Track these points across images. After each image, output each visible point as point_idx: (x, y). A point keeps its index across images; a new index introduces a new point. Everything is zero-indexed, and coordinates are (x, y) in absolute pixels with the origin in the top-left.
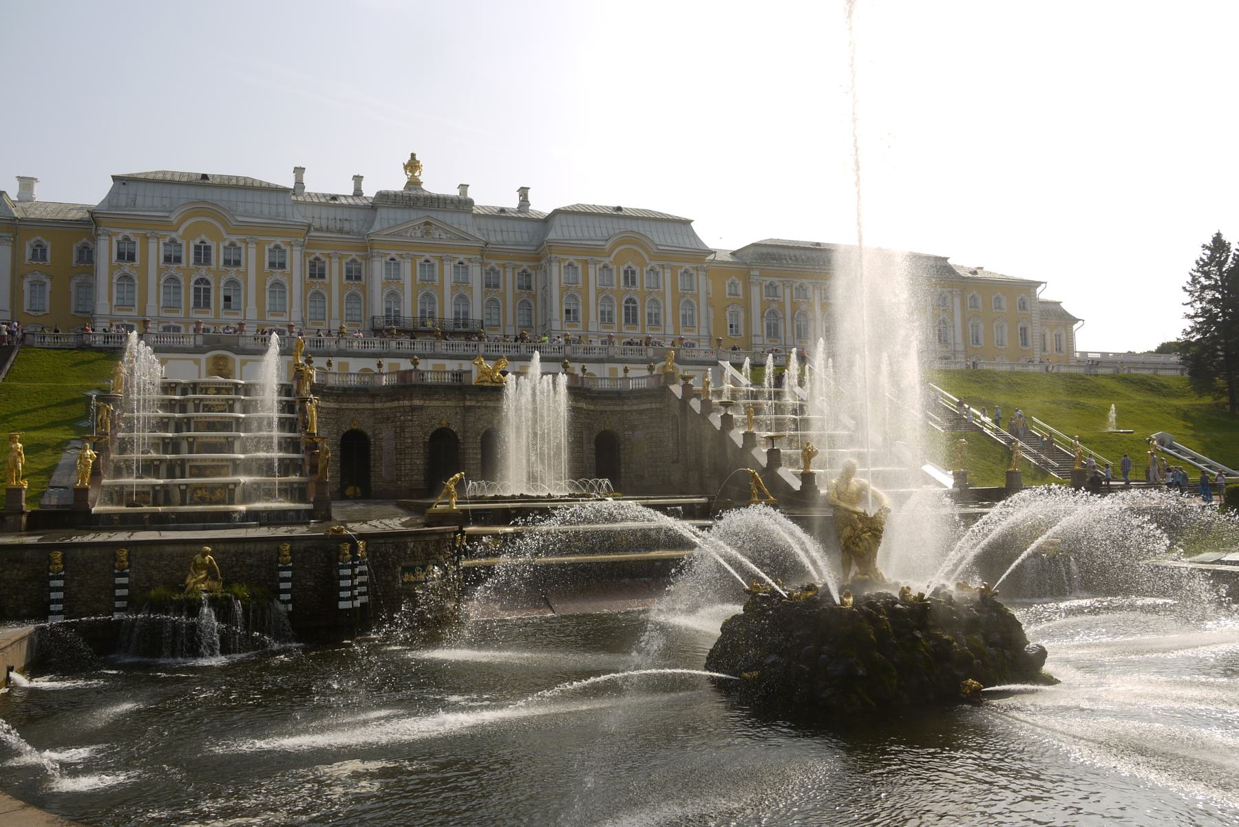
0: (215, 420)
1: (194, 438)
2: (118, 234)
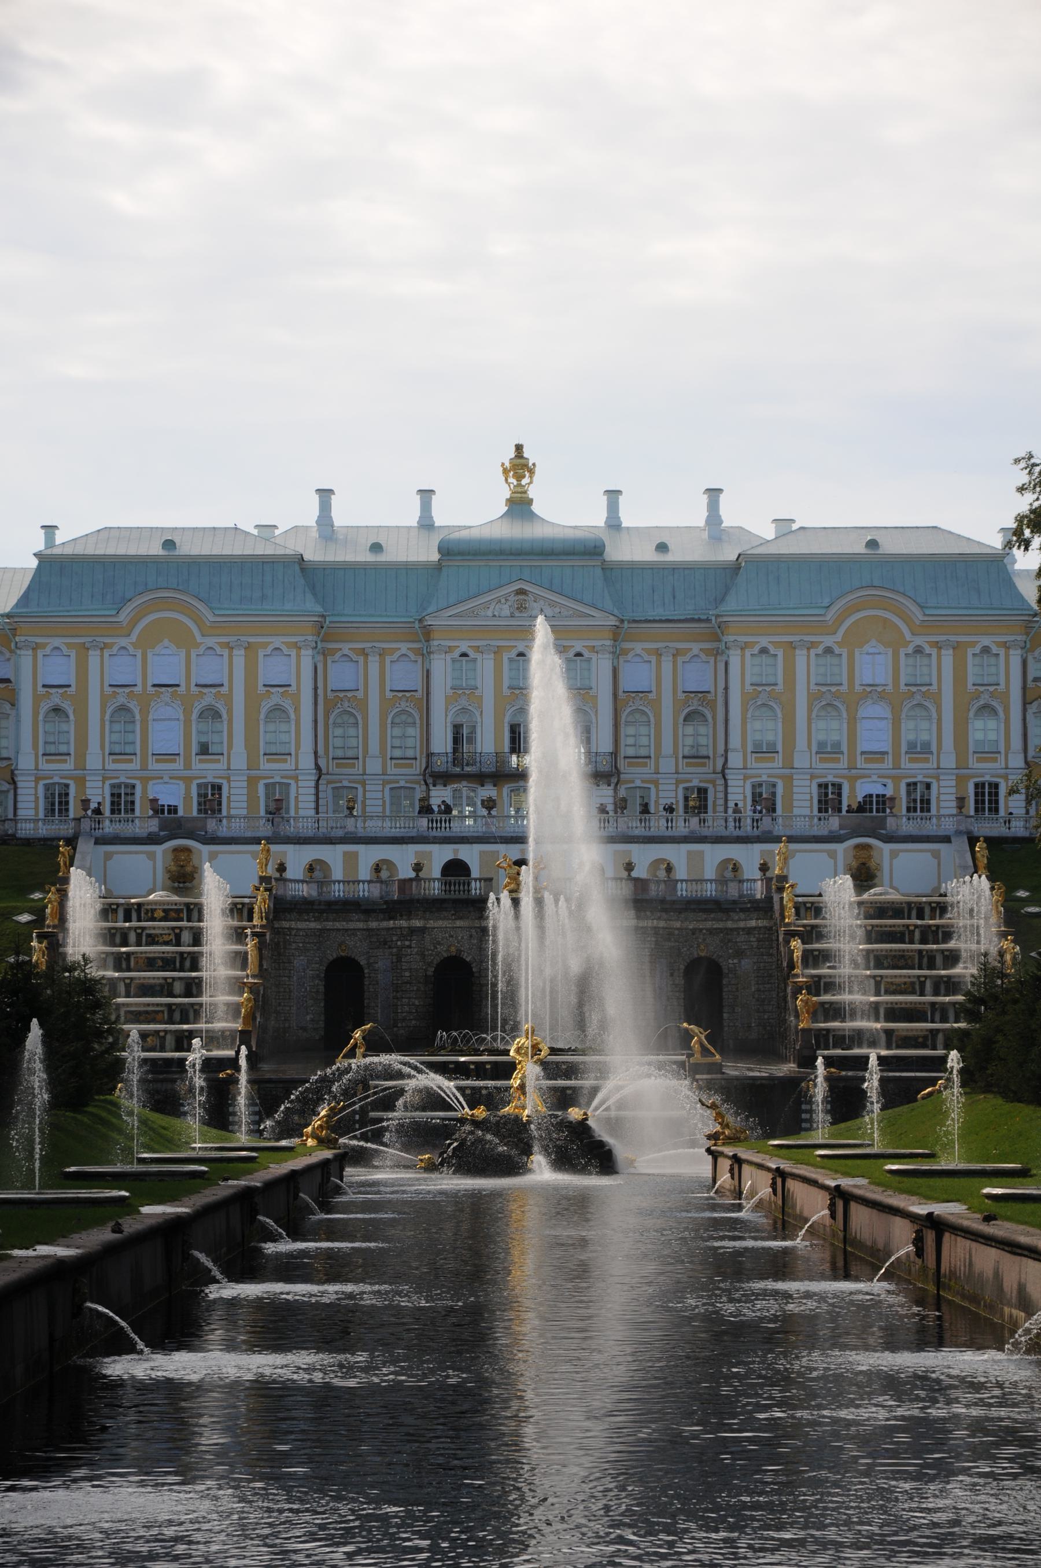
0: (157, 955)
1: (132, 979)
2: (44, 646)
